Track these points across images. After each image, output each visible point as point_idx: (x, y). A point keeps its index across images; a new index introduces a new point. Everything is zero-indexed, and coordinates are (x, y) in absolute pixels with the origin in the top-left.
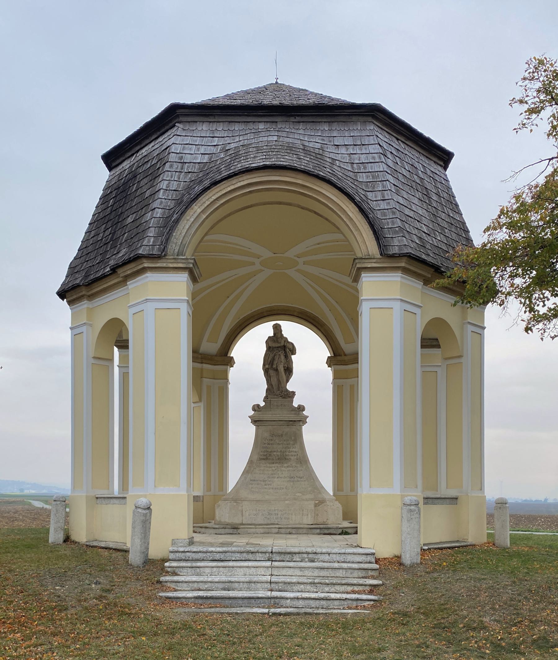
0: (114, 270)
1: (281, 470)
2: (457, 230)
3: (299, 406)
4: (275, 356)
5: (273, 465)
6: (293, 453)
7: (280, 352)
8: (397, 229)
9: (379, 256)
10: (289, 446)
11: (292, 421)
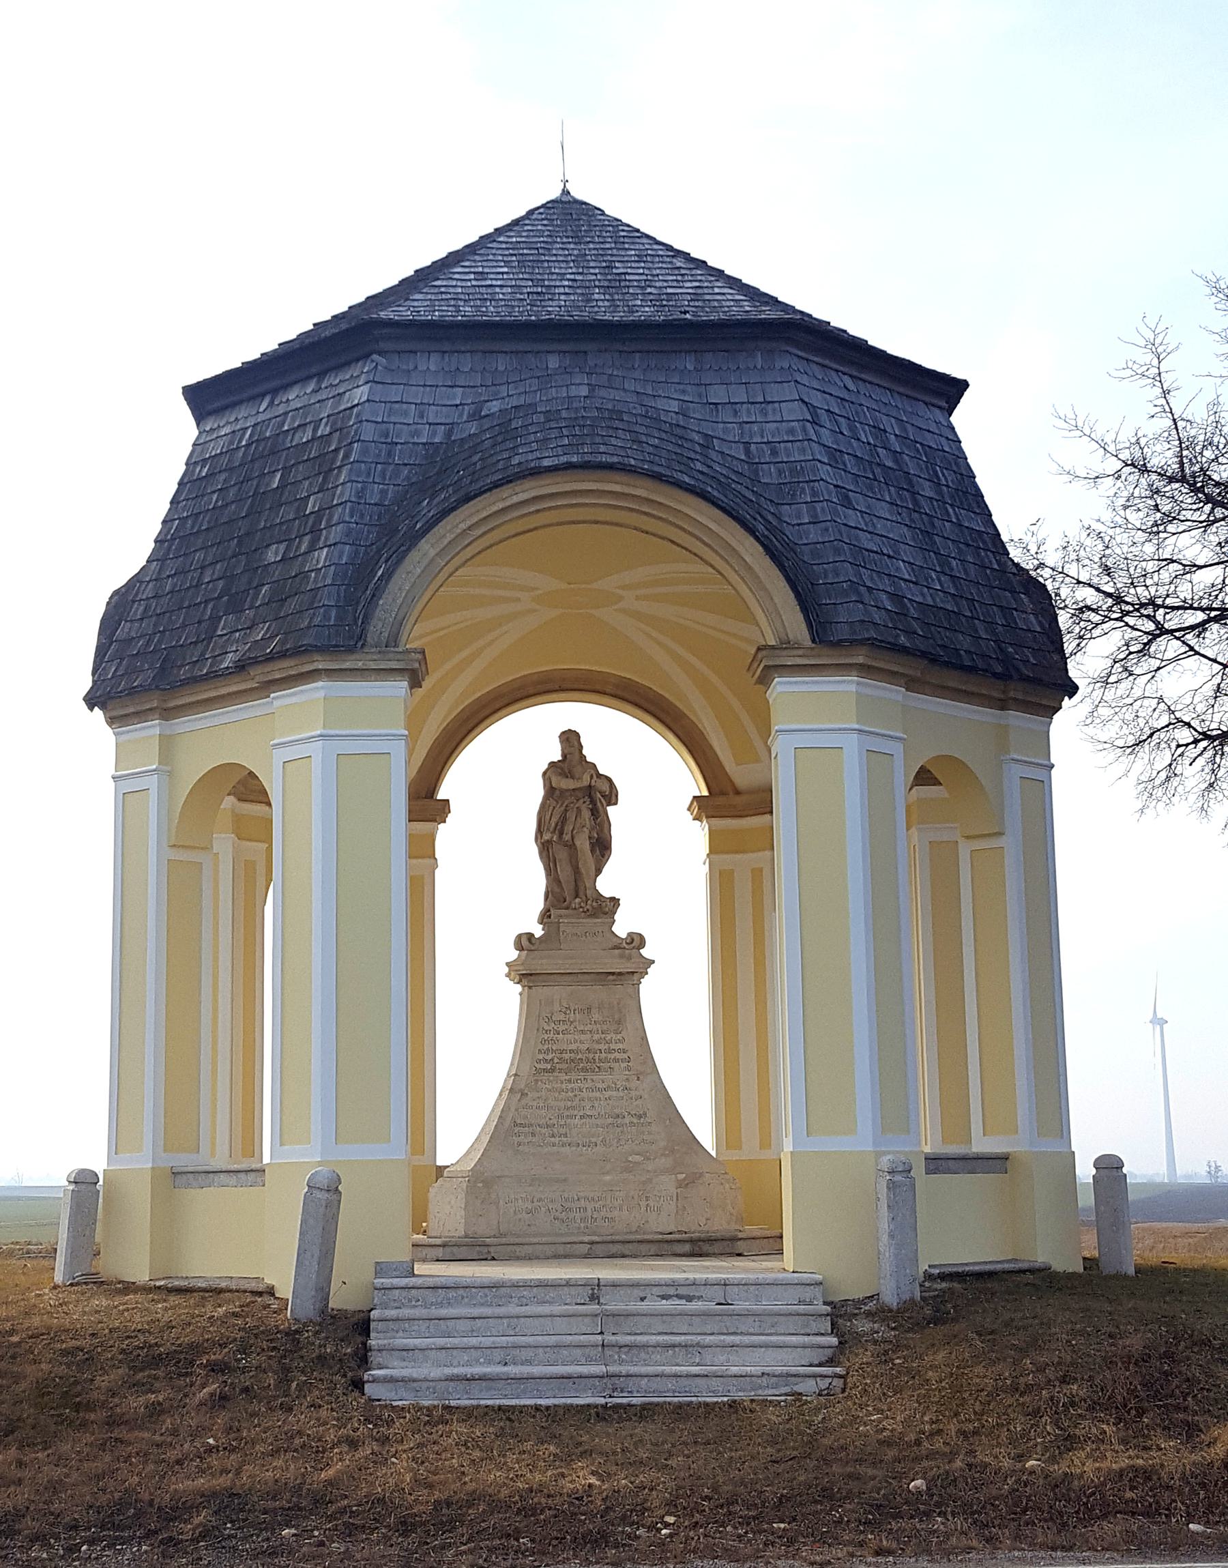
0: (241, 667)
2: (979, 555)
3: (631, 935)
4: (566, 811)
8: (845, 584)
9: (808, 643)
11: (613, 974)
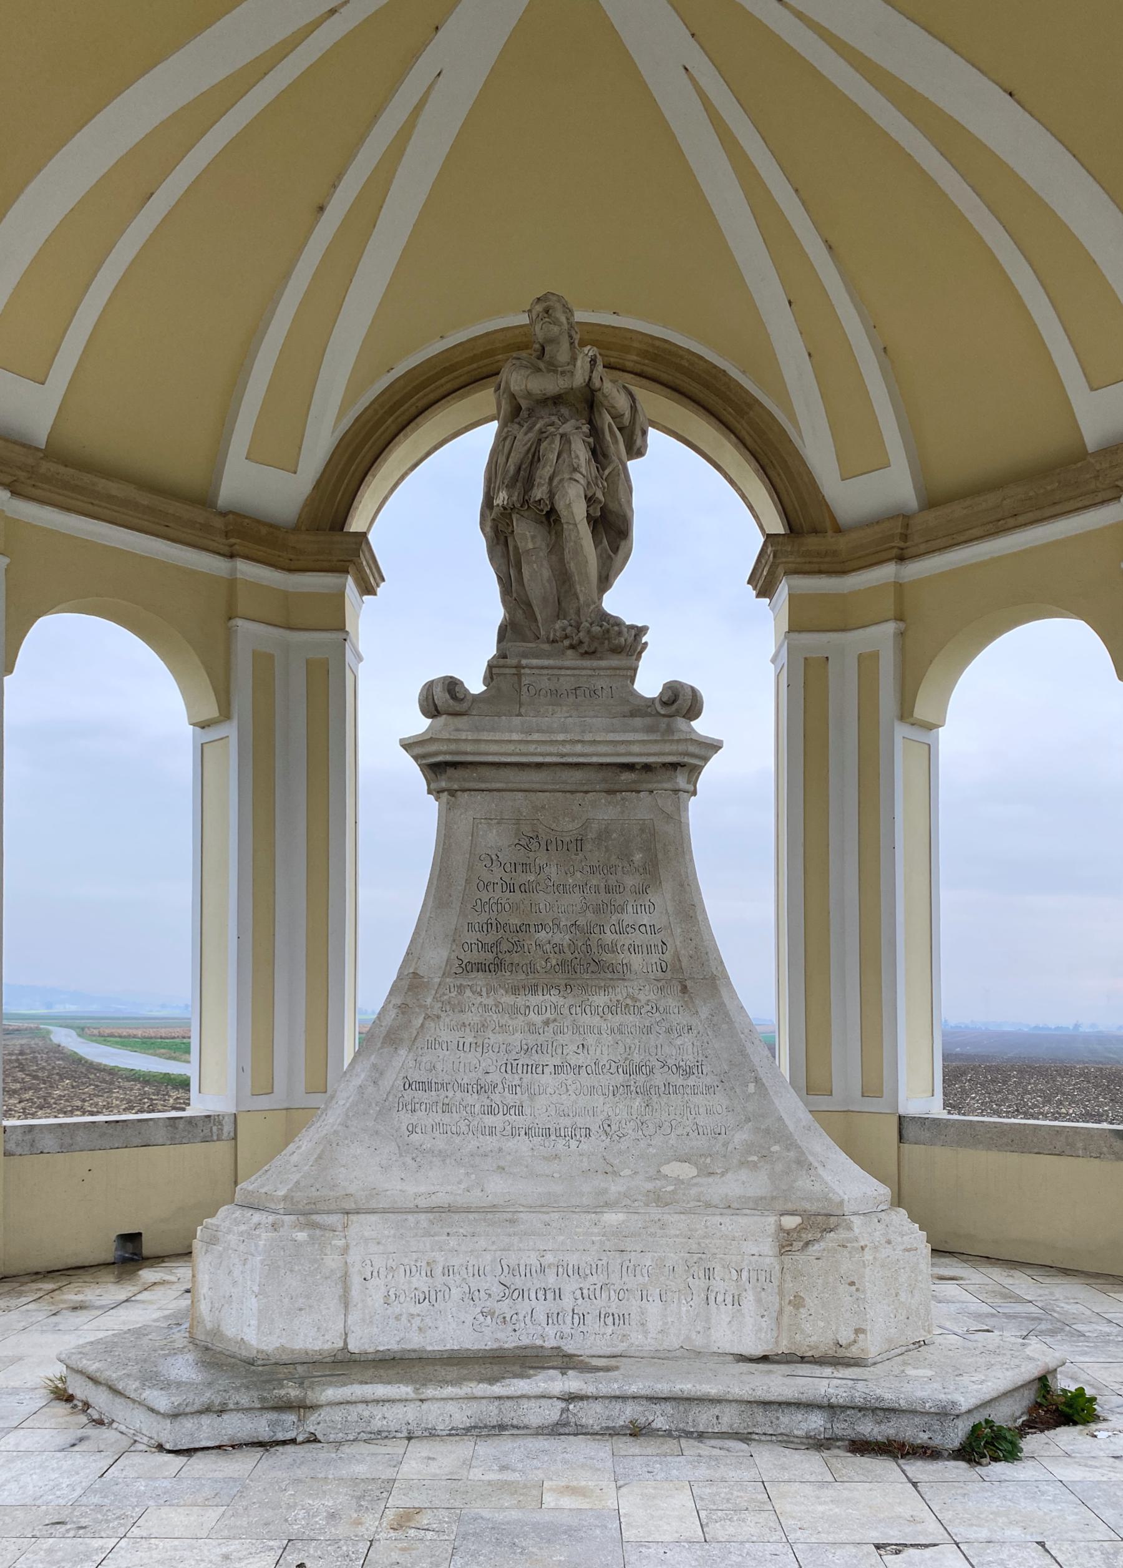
1: (577, 1029)
5: (534, 1000)
6: (639, 938)
7: (567, 428)
10: (619, 899)
11: (630, 767)
